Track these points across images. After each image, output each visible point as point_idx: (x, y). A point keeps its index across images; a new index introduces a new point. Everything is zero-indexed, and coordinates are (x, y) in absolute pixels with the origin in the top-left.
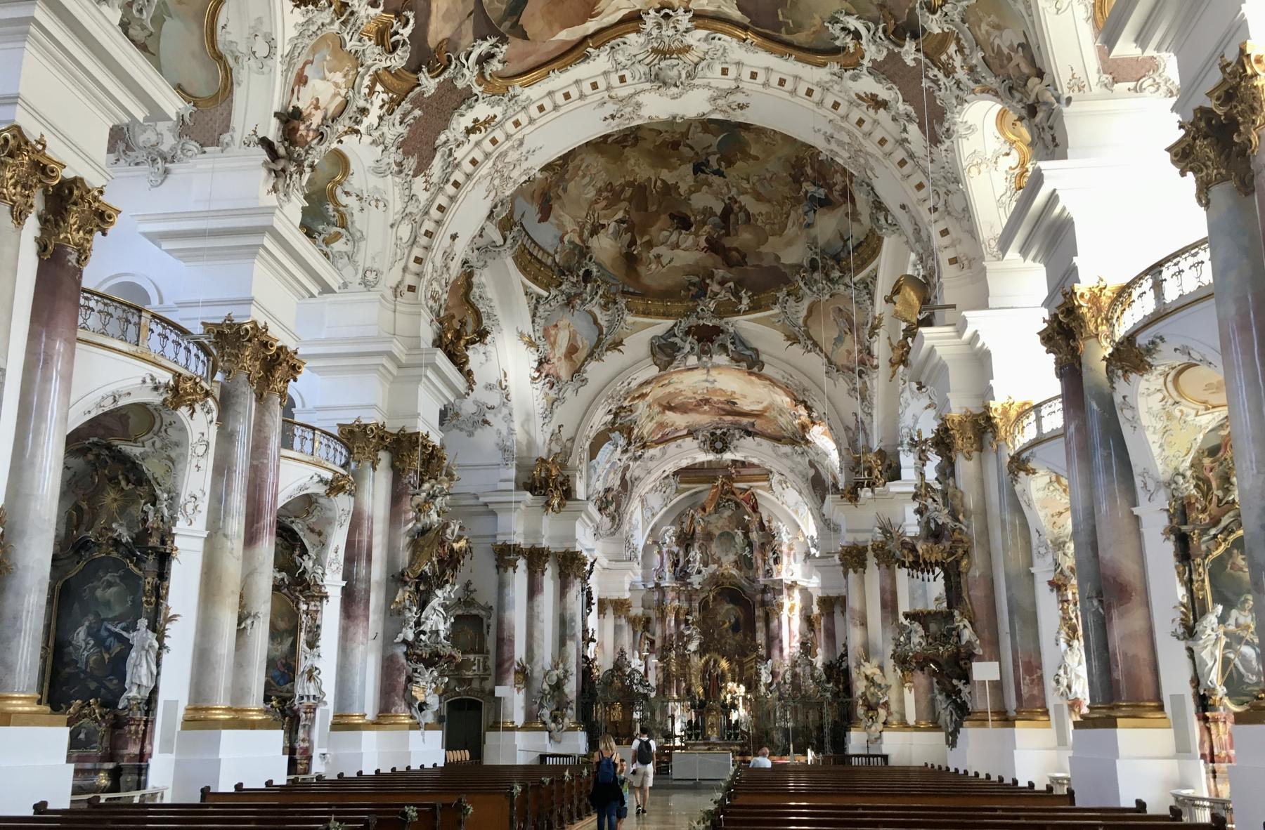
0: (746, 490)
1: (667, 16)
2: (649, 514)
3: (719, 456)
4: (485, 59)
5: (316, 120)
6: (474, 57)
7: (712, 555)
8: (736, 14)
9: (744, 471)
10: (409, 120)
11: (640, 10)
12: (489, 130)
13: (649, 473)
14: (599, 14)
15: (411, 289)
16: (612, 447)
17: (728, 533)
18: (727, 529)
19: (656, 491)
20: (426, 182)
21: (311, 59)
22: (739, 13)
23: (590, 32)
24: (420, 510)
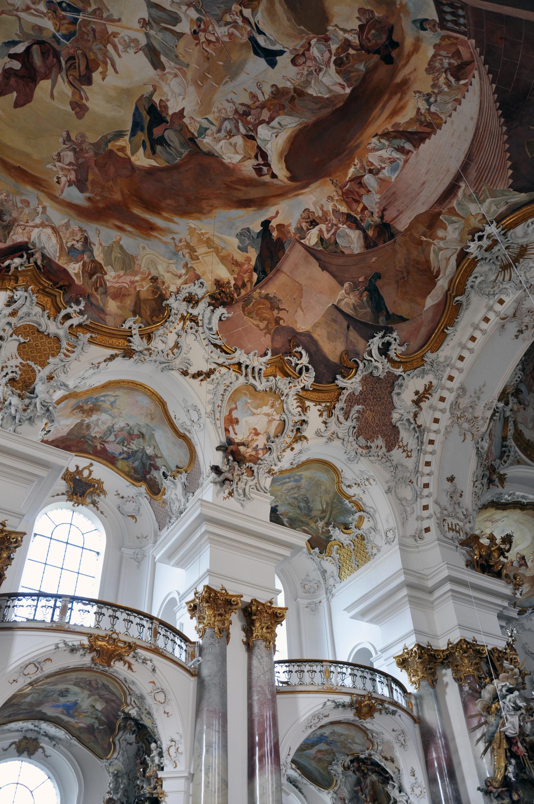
1: (480, 238)
4: (384, 350)
5: (261, 441)
6: (375, 352)
8: (522, 197)
10: (353, 413)
11: (462, 249)
12: (434, 395)
14: (438, 272)
15: (427, 530)
20: (404, 451)
21: (234, 406)
22: (523, 194)
23: (446, 286)
24: (489, 713)
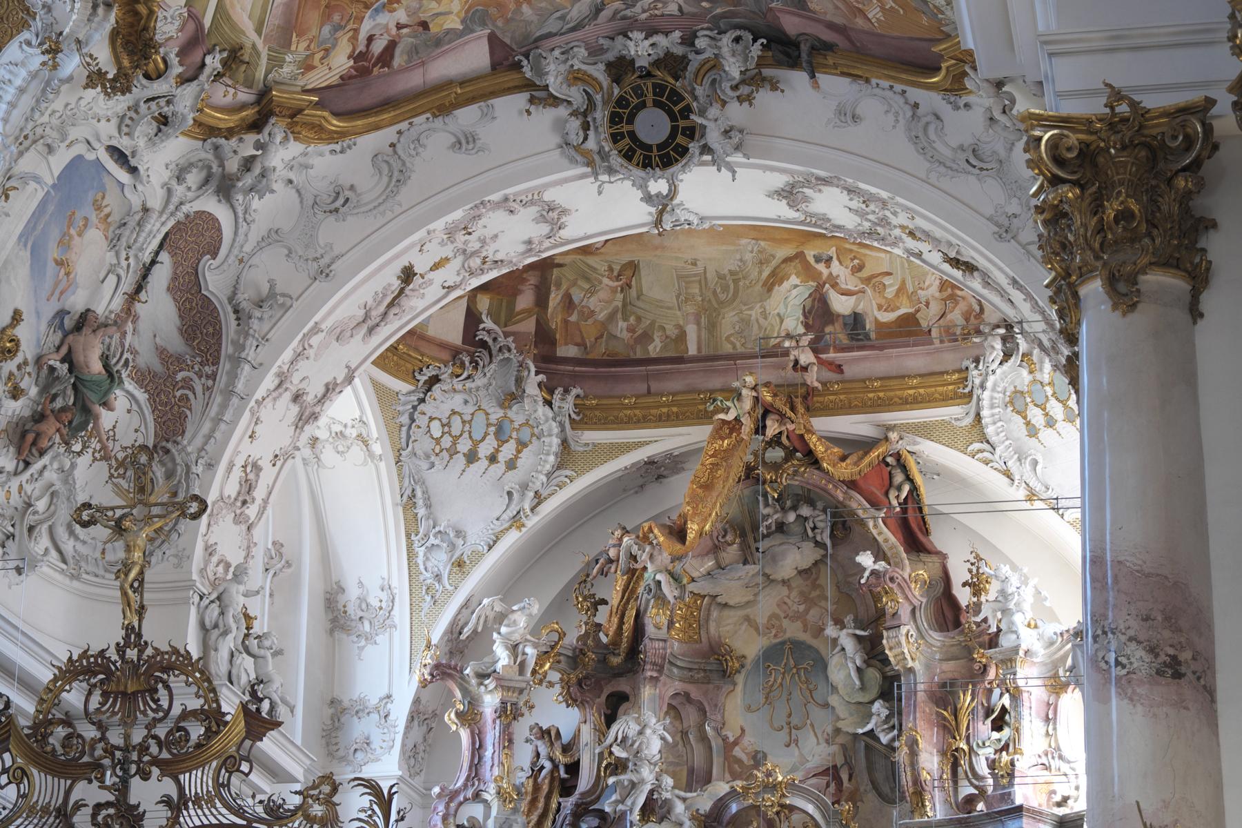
0: (865, 445)
2: (441, 560)
3: (659, 186)
7: (728, 746)
9: (860, 364)
13: (324, 273)
16: (37, 59)
17: (797, 647)
18: (794, 631)
19: (471, 457)
